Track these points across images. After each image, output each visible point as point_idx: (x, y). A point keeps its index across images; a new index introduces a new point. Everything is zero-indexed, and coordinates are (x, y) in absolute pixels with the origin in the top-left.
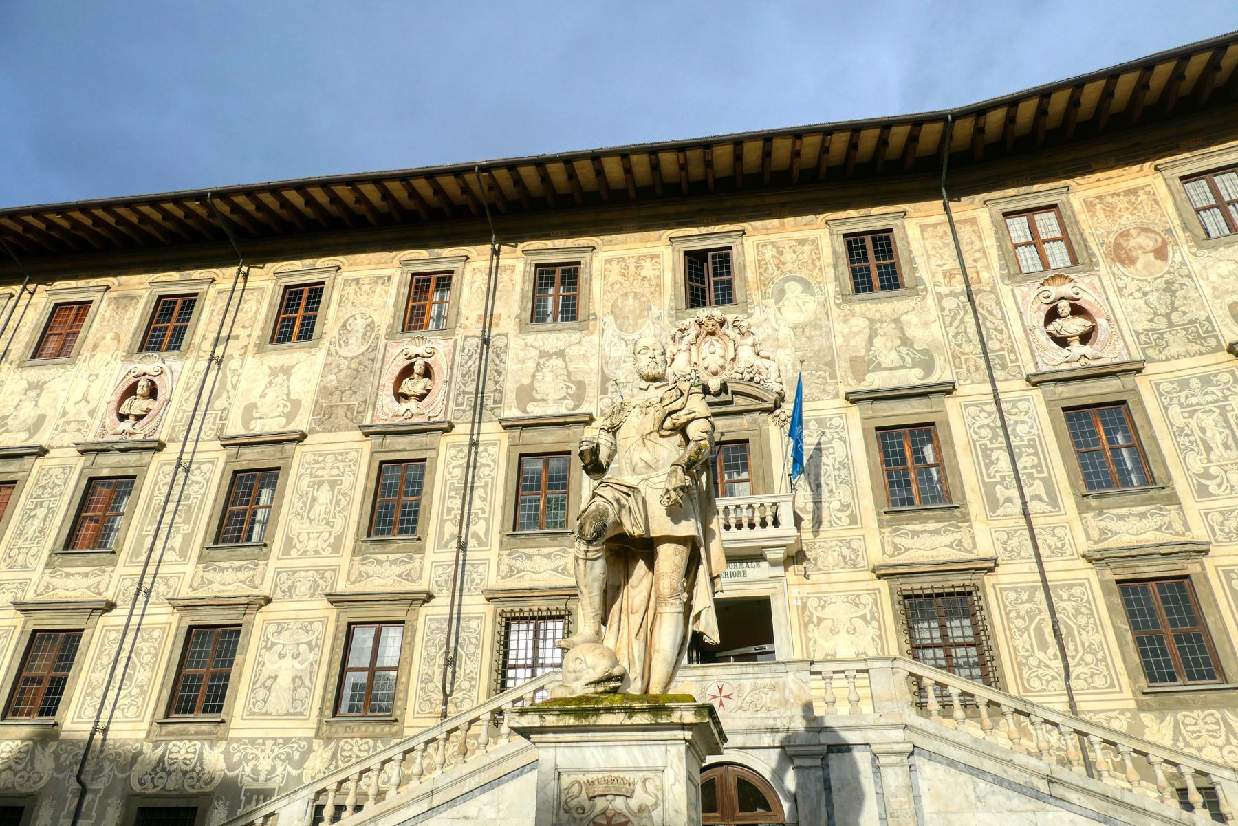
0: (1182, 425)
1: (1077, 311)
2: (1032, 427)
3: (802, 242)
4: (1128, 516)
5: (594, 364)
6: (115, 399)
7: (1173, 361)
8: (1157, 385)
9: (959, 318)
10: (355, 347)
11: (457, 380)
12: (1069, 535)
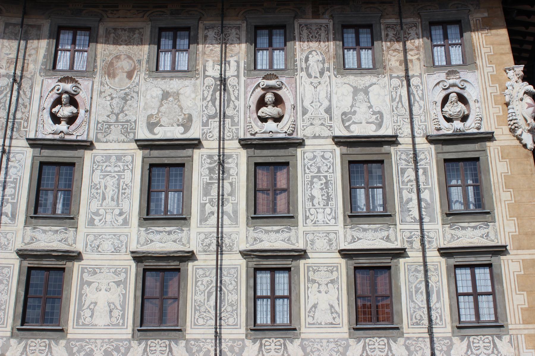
0: (97, 182)
2: (18, 171)
4: (48, 231)
7: (109, 144)
8: (95, 156)
9: (5, 92)
12: (14, 239)
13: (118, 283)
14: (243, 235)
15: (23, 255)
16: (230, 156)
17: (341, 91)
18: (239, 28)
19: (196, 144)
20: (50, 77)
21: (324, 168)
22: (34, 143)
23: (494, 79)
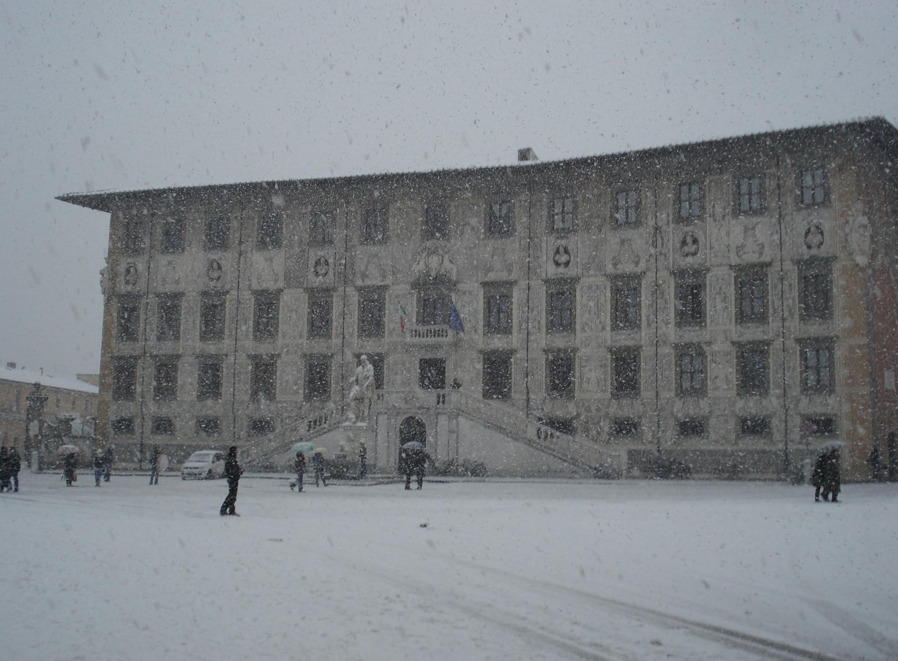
17: (736, 227)
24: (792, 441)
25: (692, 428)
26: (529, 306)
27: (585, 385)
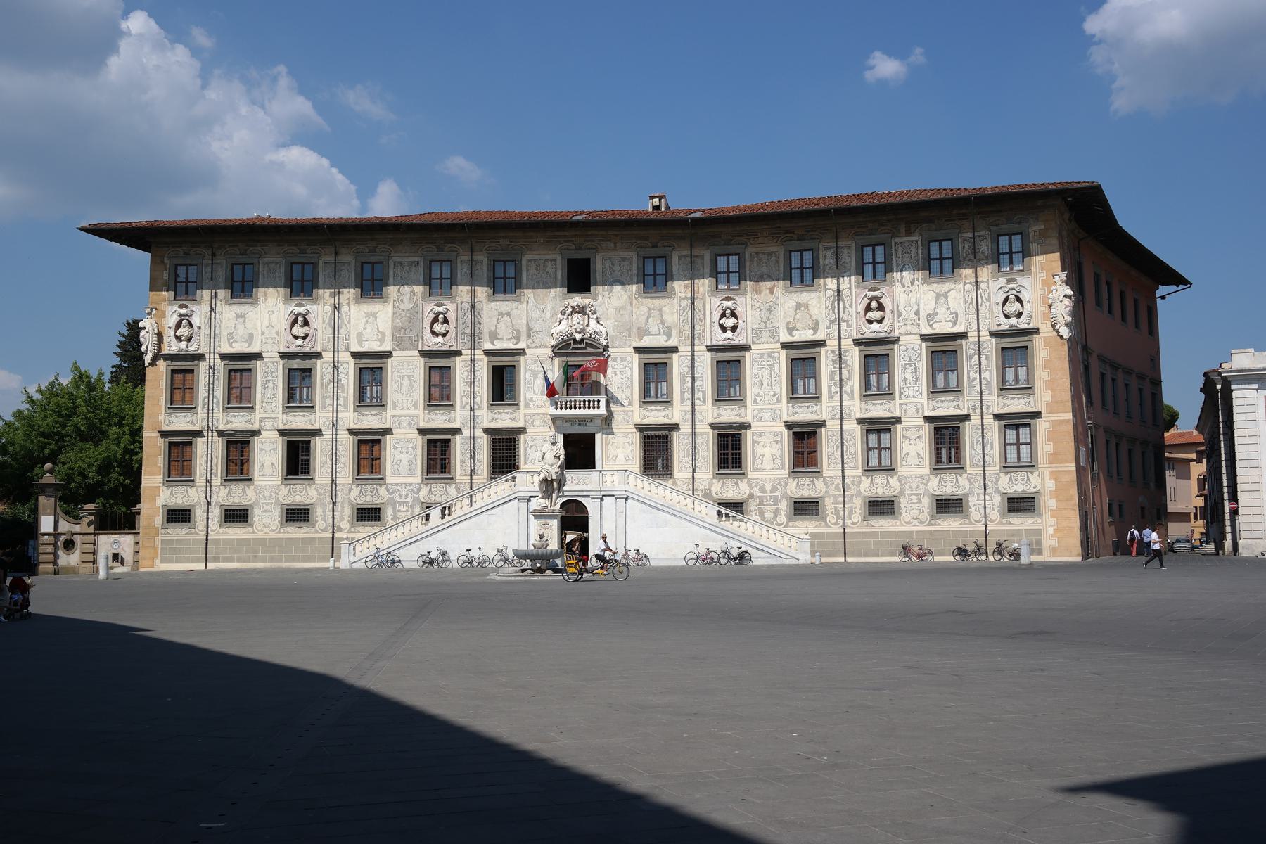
1: (733, 315)
3: (624, 259)
5: (524, 321)
6: (288, 327)
10: (407, 305)
11: (460, 327)
13: (777, 442)
14: (857, 408)
15: (714, 426)
16: (846, 351)
18: (849, 248)
19: (821, 344)
20: (715, 296)
21: (914, 358)
22: (711, 349)
23: (1044, 283)
24: (991, 521)
25: (880, 507)
26: (691, 373)
27: (759, 462)
